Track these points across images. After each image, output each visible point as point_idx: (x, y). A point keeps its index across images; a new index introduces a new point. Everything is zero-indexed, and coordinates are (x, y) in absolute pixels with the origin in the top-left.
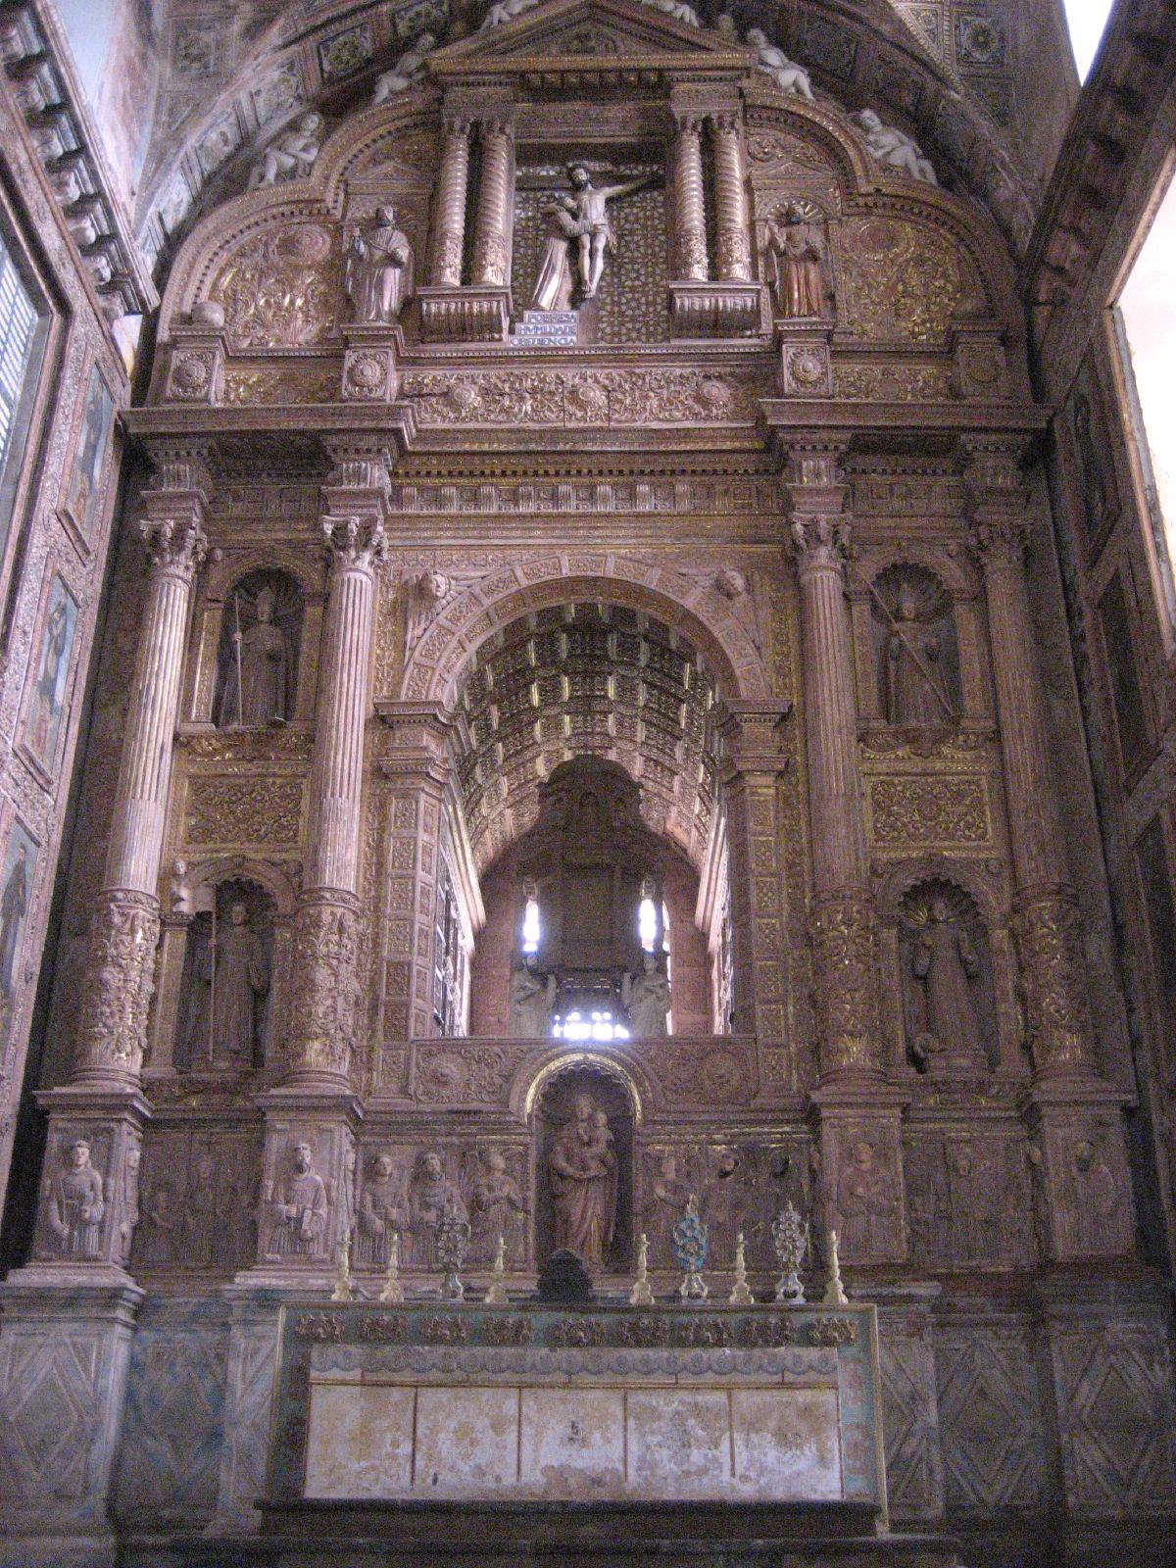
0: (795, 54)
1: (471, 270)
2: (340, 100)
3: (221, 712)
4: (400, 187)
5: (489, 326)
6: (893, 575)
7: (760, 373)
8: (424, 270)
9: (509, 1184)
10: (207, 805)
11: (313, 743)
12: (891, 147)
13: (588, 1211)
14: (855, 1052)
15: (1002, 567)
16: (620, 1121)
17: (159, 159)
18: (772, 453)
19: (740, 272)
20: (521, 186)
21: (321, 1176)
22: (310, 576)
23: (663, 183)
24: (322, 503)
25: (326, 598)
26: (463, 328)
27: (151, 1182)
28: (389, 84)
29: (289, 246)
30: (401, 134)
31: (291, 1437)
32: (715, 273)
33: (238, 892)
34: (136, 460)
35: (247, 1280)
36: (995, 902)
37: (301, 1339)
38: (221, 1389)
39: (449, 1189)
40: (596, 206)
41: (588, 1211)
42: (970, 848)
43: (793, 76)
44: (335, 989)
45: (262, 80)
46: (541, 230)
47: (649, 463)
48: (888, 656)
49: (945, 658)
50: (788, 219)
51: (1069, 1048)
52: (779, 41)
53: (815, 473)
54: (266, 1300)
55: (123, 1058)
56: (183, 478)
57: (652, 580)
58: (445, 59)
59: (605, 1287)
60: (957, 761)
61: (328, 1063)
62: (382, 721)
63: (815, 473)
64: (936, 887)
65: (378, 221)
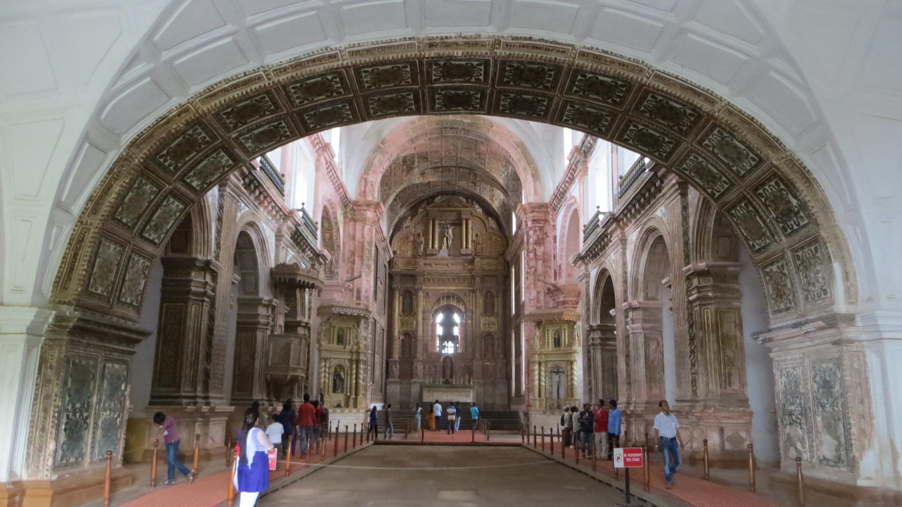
0: (481, 206)
1: (433, 247)
2: (413, 210)
3: (403, 311)
4: (422, 228)
5: (435, 255)
6: (488, 292)
7: (472, 262)
8: (427, 245)
9: (440, 369)
10: (403, 324)
11: (416, 314)
12: (492, 223)
13: (448, 372)
14: (478, 356)
15: (501, 294)
16: (452, 363)
17: (389, 229)
18: (473, 277)
19: (470, 246)
20: (440, 224)
21: (419, 368)
22: (413, 292)
23: (460, 225)
24: (415, 283)
25: (416, 295)
26: (432, 255)
27: (400, 369)
28: (420, 210)
29: (407, 238)
30: (422, 218)
31: (421, 396)
32: (467, 247)
33: (406, 334)
34: (391, 276)
35: (413, 380)
36: (496, 337)
37: (421, 388)
38: (410, 391)
39: (433, 370)
40: (450, 231)
41: (448, 372)
42: (494, 329)
43: (480, 210)
44: (420, 347)
45: (402, 212)
46: (442, 236)
47: (457, 278)
48: (485, 304)
49: (493, 305)
50: (477, 236)
51: (501, 356)
52: (478, 203)
53: (478, 280)
54: (415, 382)
55: (396, 356)
56: (397, 279)
57: (456, 293)
58: (428, 208)
59: (450, 380)
60: (492, 319)
61: (420, 356)
62: (424, 312)
63: (478, 280)
64: (489, 335)
65: (419, 235)
